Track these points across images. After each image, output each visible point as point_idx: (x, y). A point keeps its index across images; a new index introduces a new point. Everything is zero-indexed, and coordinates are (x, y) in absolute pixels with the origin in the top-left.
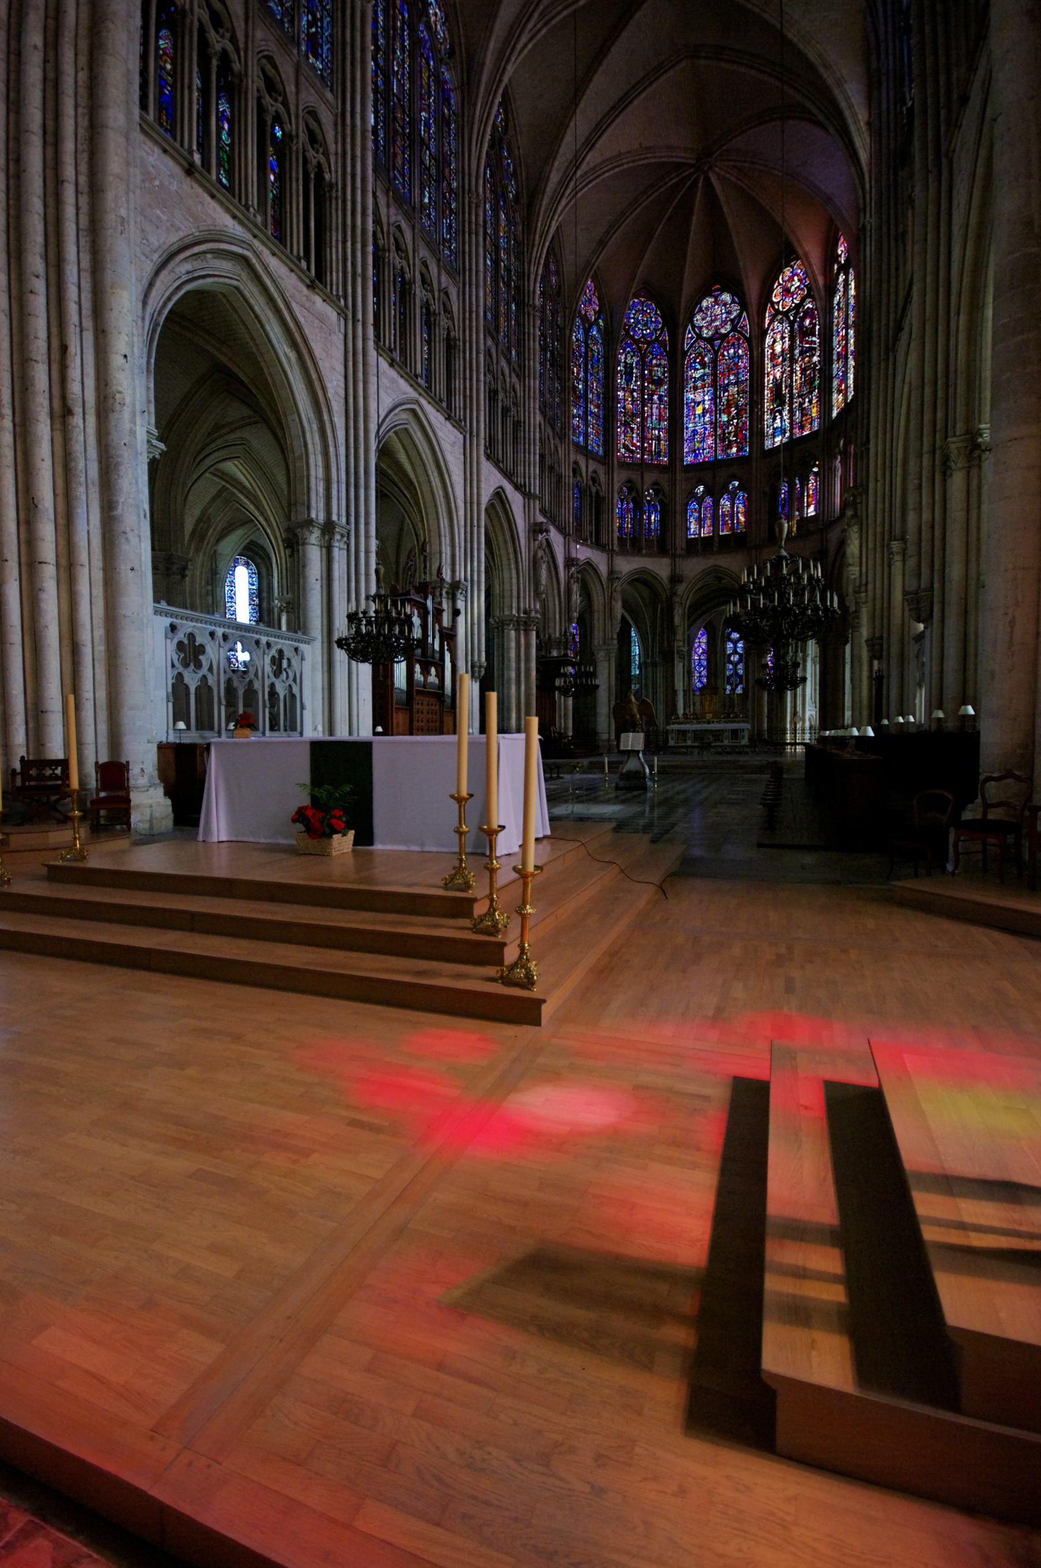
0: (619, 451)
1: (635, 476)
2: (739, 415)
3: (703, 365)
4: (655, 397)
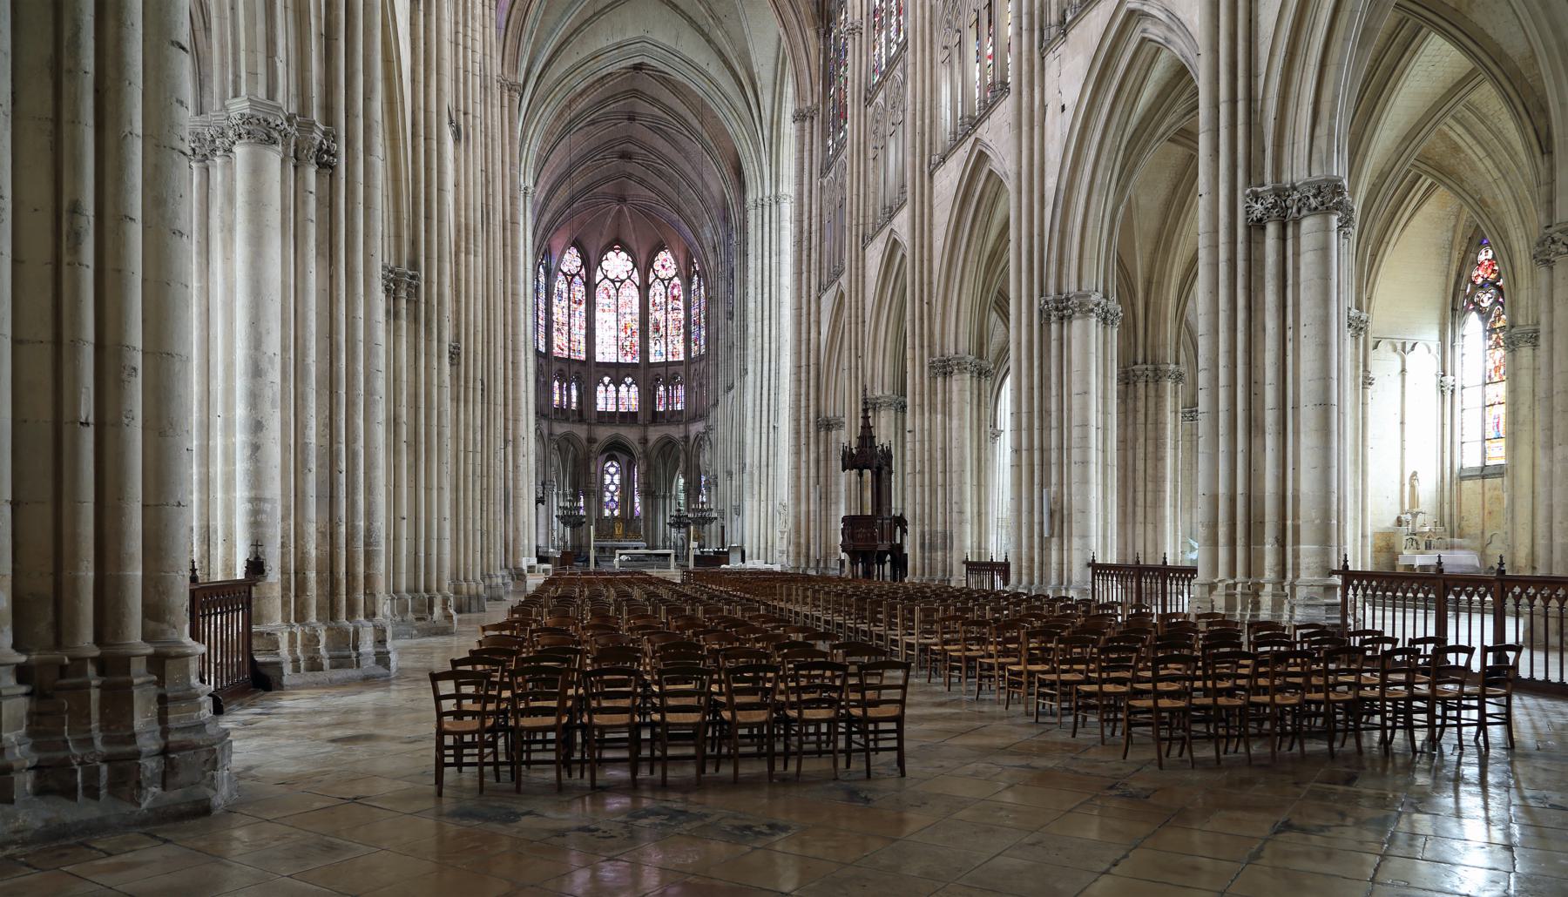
0: (552, 348)
1: (565, 368)
2: (633, 333)
3: (609, 297)
4: (577, 313)
